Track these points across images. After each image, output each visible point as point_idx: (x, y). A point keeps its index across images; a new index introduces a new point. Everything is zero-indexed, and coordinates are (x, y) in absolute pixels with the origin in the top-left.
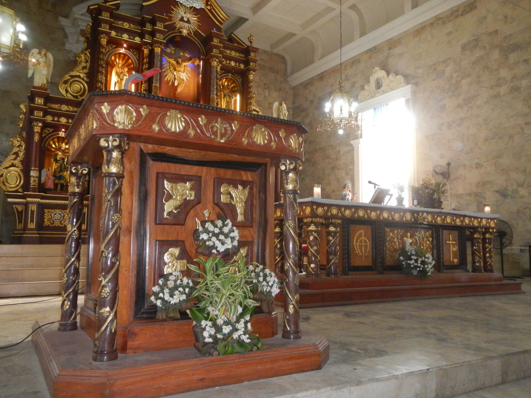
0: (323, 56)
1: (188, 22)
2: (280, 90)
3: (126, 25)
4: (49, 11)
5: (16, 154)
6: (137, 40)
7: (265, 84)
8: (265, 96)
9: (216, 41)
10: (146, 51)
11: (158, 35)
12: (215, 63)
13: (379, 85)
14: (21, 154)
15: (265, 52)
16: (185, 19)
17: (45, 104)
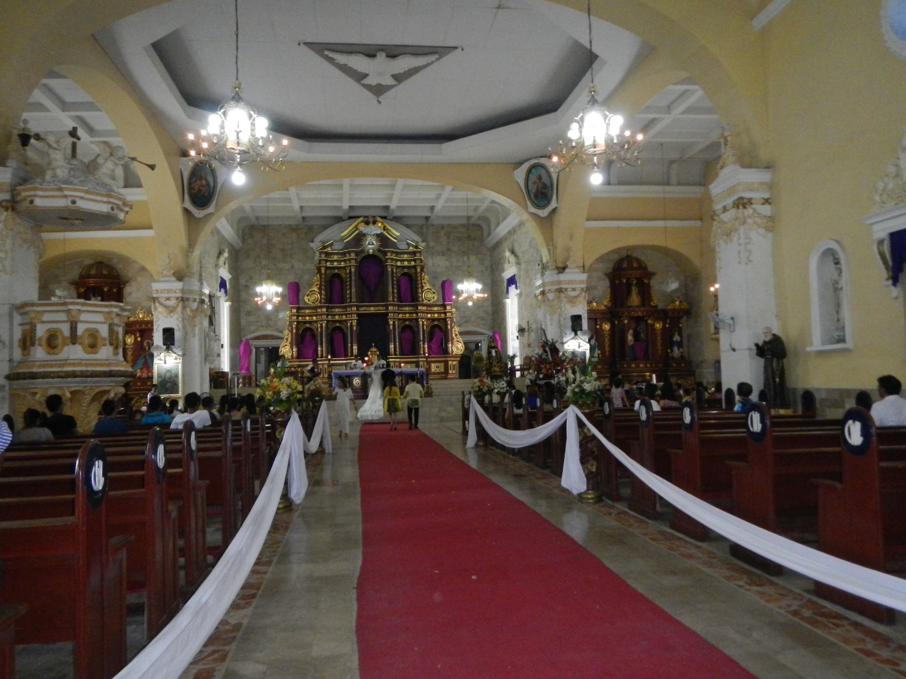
0: (494, 231)
1: (373, 244)
2: (478, 253)
3: (335, 257)
4: (303, 238)
5: (287, 339)
6: (343, 264)
7: (463, 252)
8: (464, 262)
9: (389, 254)
10: (348, 271)
11: (352, 261)
12: (390, 269)
13: (509, 263)
14: (289, 339)
15: (462, 225)
16: (371, 243)
17: (297, 312)
